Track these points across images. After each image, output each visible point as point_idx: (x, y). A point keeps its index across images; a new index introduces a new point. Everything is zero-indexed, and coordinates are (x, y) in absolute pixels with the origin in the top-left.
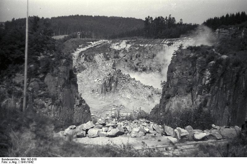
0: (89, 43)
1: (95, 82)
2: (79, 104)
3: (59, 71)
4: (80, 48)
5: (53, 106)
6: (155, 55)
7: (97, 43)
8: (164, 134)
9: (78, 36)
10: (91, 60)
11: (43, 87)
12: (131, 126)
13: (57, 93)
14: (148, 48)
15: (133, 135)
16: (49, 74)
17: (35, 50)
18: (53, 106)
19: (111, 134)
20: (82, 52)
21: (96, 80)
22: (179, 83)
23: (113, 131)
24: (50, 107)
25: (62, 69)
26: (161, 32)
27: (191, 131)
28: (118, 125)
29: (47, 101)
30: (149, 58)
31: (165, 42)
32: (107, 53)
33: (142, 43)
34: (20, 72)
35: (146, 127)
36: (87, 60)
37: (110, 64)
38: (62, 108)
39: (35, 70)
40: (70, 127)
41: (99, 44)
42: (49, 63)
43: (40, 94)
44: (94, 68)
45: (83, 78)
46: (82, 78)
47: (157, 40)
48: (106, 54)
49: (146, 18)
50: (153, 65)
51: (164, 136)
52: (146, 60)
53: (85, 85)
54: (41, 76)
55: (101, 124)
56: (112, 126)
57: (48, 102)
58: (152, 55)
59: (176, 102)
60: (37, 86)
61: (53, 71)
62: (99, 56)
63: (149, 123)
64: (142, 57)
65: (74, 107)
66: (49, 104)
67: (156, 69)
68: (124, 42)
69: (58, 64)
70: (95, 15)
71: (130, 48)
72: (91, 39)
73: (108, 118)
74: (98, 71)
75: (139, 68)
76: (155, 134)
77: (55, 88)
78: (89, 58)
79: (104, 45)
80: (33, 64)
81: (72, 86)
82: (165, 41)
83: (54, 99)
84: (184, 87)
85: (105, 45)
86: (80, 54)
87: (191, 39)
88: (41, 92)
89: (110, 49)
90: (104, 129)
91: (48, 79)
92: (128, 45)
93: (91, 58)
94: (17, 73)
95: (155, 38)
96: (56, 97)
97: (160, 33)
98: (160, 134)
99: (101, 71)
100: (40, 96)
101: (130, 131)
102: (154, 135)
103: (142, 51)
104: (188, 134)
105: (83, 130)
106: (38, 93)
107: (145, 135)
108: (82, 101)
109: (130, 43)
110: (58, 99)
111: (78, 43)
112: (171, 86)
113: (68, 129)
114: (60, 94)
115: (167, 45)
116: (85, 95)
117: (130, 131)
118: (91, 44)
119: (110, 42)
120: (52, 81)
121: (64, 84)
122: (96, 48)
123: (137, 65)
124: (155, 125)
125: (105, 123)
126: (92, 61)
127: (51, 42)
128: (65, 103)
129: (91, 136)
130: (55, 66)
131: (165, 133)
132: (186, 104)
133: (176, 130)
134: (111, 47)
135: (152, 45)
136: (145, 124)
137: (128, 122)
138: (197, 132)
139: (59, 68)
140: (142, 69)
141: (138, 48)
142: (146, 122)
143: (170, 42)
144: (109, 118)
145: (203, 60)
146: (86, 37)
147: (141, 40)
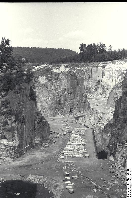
1: (45, 100)
2: (39, 121)
5: (17, 123)
7: (40, 67)
10: (36, 81)
13: (20, 109)
14: (85, 70)
21: (46, 98)
24: (13, 124)
26: (95, 57)
30: (86, 79)
31: (100, 65)
32: (49, 76)
33: (79, 66)
41: (42, 68)
49: (81, 45)
50: (89, 85)
58: (88, 76)
62: (42, 78)
69: (19, 81)
70: (32, 47)
72: (34, 64)
73: (65, 133)
74: (47, 90)
82: (99, 64)
89: (52, 72)
95: (90, 62)
96: (19, 114)
99: (50, 90)
103: (79, 73)
108: (43, 118)
109: (68, 66)
114: (23, 111)
115: (101, 68)
118: (35, 68)
120: (14, 98)
128: (27, 120)
130: (17, 84)
134: (52, 70)
135: (88, 68)
139: (21, 84)
141: (76, 71)
143: (103, 65)
144: (66, 134)
147: (77, 64)
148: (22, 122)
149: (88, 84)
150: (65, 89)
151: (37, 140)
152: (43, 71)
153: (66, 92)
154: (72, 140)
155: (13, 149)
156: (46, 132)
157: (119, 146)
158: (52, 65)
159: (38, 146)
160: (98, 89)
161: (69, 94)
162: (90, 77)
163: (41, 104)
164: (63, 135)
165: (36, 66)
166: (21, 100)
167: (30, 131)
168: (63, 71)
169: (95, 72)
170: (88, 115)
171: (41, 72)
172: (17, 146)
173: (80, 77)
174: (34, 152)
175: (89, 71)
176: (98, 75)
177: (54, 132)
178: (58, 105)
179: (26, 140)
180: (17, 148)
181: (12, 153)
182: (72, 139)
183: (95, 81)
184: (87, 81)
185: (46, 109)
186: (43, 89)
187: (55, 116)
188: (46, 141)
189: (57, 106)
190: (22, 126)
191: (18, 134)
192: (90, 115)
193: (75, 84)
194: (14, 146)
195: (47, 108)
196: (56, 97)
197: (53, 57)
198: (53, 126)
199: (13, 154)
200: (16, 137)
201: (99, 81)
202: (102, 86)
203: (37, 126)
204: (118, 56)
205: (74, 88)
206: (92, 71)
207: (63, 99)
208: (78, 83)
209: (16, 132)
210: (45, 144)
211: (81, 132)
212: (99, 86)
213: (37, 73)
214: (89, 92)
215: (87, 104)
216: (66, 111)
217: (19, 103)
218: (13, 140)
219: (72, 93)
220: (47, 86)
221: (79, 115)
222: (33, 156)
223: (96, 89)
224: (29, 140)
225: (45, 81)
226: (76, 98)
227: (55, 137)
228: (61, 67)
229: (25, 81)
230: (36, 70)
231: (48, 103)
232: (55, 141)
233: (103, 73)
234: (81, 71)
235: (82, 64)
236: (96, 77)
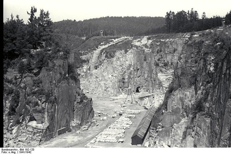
0: (110, 40)
1: (109, 78)
4: (102, 45)
5: (47, 104)
6: (177, 49)
7: (119, 40)
9: (101, 35)
10: (112, 56)
11: (37, 83)
14: (169, 43)
17: (28, 43)
18: (47, 104)
20: (103, 49)
21: (111, 75)
22: (182, 74)
24: (44, 105)
25: (58, 62)
29: (40, 99)
30: (170, 53)
31: (187, 36)
33: (163, 38)
36: (107, 57)
38: (58, 106)
39: (28, 65)
41: (121, 40)
45: (98, 74)
46: (97, 74)
50: (174, 60)
52: (167, 55)
53: (100, 81)
54: (35, 71)
57: (41, 100)
58: (173, 50)
60: (31, 82)
61: (47, 66)
64: (163, 52)
65: (75, 105)
68: (145, 38)
69: (54, 57)
70: (125, 16)
72: (113, 36)
73: (115, 115)
75: (160, 63)
78: (110, 55)
79: (126, 42)
83: (48, 96)
84: (188, 77)
86: (102, 51)
88: (35, 88)
91: (44, 73)
92: (150, 40)
93: (112, 55)
96: (50, 94)
99: (116, 66)
100: (34, 93)
103: (163, 46)
106: (32, 90)
109: (151, 38)
111: (100, 40)
116: (99, 91)
118: (113, 41)
119: (131, 38)
121: (60, 78)
123: (159, 60)
128: (61, 100)
132: (189, 98)
134: (132, 43)
139: (55, 61)
140: (163, 65)
141: (159, 43)
144: (116, 116)
145: (210, 44)
146: (108, 35)
148: (54, 102)
149: (173, 58)
150: (130, 66)
151: (74, 123)
152: (123, 44)
153: (132, 69)
154: (117, 123)
155: (40, 132)
156: (86, 113)
157: (152, 130)
158: (132, 38)
159: (74, 129)
161: (135, 70)
164: (112, 117)
165: (115, 39)
166: (53, 79)
167: (65, 113)
168: (145, 44)
170: (157, 95)
172: (45, 128)
173: (149, 51)
174: (67, 136)
175: (174, 43)
177: (104, 114)
178: (121, 83)
179: (59, 122)
180: (45, 131)
181: (39, 136)
182: (118, 122)
184: (172, 55)
185: (110, 88)
186: (108, 65)
187: (117, 96)
188: (86, 124)
189: (120, 84)
190: (53, 107)
191: (48, 115)
192: (160, 95)
193: (143, 60)
194: (42, 128)
195: (111, 87)
196: (120, 74)
197: (149, 26)
198: (108, 107)
199: (40, 137)
200: (46, 119)
203: (76, 107)
204: (210, 25)
205: (141, 64)
206: (178, 43)
207: (127, 77)
208: (145, 58)
209: (46, 113)
210: (85, 127)
211: (134, 114)
214: (173, 68)
215: (158, 82)
216: (132, 90)
217: (51, 82)
218: (42, 123)
219: (139, 70)
220: (113, 62)
221: (146, 95)
222: (64, 140)
224: (64, 123)
226: (144, 76)
227: (101, 119)
229: (61, 57)
230: (114, 43)
231: (112, 81)
232: (97, 124)
234: (165, 43)
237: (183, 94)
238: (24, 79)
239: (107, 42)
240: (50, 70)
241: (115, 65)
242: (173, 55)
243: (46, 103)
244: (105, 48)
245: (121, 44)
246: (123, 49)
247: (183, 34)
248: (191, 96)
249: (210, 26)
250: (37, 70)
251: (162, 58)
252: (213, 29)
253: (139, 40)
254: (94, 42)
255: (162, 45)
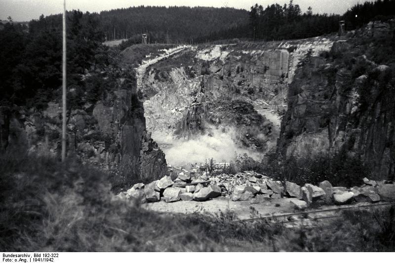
0: (161, 50)
1: (172, 114)
3: (115, 97)
4: (148, 59)
5: (107, 153)
6: (268, 67)
7: (174, 51)
8: (285, 196)
9: (144, 41)
10: (165, 78)
11: (91, 123)
12: (232, 182)
13: (113, 132)
15: (235, 197)
16: (99, 103)
17: (77, 65)
18: (107, 153)
19: (201, 197)
20: (150, 65)
21: (174, 110)
22: (308, 113)
23: (202, 192)
24: (102, 155)
25: (120, 93)
26: (277, 30)
27: (328, 190)
28: (210, 182)
29: (97, 146)
30: (258, 72)
31: (284, 46)
34: (55, 100)
35: (256, 184)
37: (195, 85)
39: (77, 97)
40: (136, 185)
41: (178, 51)
42: (99, 85)
43: (86, 135)
44: (170, 91)
46: (151, 107)
47: (270, 42)
48: (189, 68)
50: (264, 85)
51: (284, 198)
52: (254, 76)
53: (157, 119)
54: (87, 106)
55: (184, 181)
56: (202, 183)
57: (99, 148)
59: (303, 143)
60: (83, 121)
61: (105, 97)
63: (260, 177)
64: (247, 71)
66: (102, 150)
67: (269, 90)
68: (217, 48)
69: (112, 86)
71: (226, 58)
72: (164, 45)
73: (195, 170)
74: (176, 95)
75: (243, 89)
76: (270, 196)
77: (110, 124)
78: (163, 75)
79: (185, 54)
80: (74, 87)
81: (137, 120)
82: (283, 44)
83: (108, 142)
85: (187, 53)
86: (148, 69)
87: (326, 41)
88: (88, 131)
89: (196, 60)
90: (188, 188)
93: (165, 76)
94: (50, 102)
95: (267, 40)
96: (111, 139)
97: (275, 32)
98: (279, 195)
99: (182, 95)
100: (87, 138)
101: (230, 190)
102: (269, 197)
103: (247, 62)
104: (325, 193)
105: (156, 190)
107: (254, 197)
108: (153, 144)
109: (227, 49)
110: (114, 142)
112: (294, 117)
113: (132, 189)
114: (118, 135)
115: (286, 51)
117: (230, 190)
118: (165, 52)
121: (124, 117)
122: (173, 58)
123: (239, 84)
124: (269, 180)
125: (190, 178)
126: (167, 81)
127: (101, 51)
128: (126, 148)
129: (168, 199)
131: (287, 193)
132: (319, 146)
133: (304, 188)
134: (196, 57)
136: (255, 179)
137: (227, 176)
138: (339, 191)
139: (115, 92)
141: (240, 57)
142: (256, 177)
143: (291, 46)
144: (196, 171)
145: (346, 73)
147: (244, 44)
152: (180, 57)
160: (279, 91)
162: (266, 69)
163: (165, 120)
169: (275, 59)
171: (176, 59)
176: (281, 65)
183: (275, 77)
201: (283, 76)
202: (288, 85)
212: (281, 85)
213: (168, 61)
220: (177, 88)
223: (276, 92)
225: (182, 76)
228: (212, 49)
229: (123, 87)
230: (166, 56)
233: (289, 61)
234: (249, 57)
235: (253, 45)
236: (276, 69)
237: (310, 140)
238: (72, 117)
239: (155, 54)
240: (110, 105)
241: (180, 94)
242: (263, 76)
243: (106, 153)
244: (152, 64)
245: (178, 58)
246: (182, 66)
247: (277, 43)
248: (322, 144)
249: (320, 31)
250: (90, 105)
251: (244, 81)
252: (325, 36)
253: (207, 50)
254: (135, 54)
255: (245, 60)
